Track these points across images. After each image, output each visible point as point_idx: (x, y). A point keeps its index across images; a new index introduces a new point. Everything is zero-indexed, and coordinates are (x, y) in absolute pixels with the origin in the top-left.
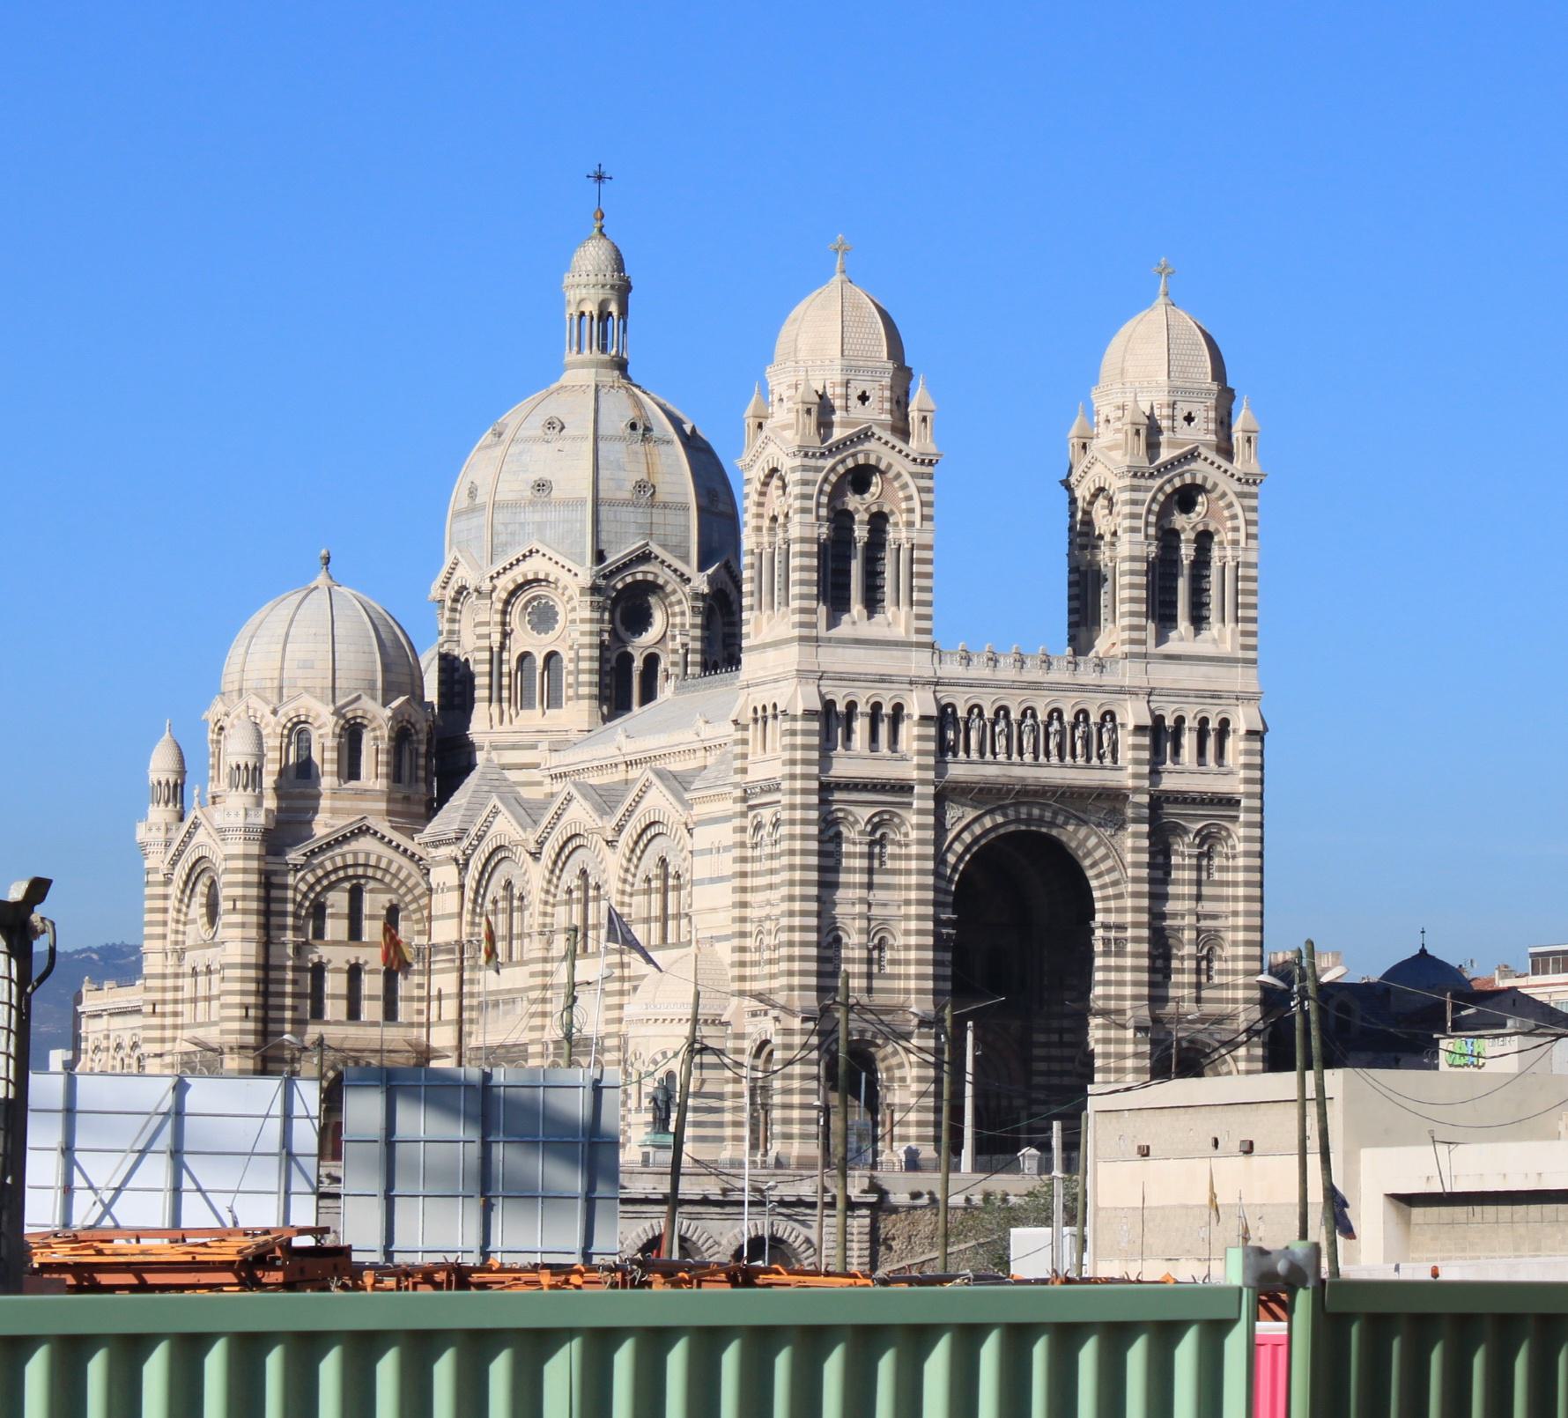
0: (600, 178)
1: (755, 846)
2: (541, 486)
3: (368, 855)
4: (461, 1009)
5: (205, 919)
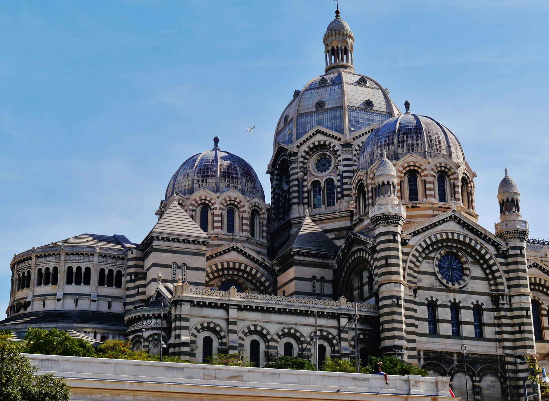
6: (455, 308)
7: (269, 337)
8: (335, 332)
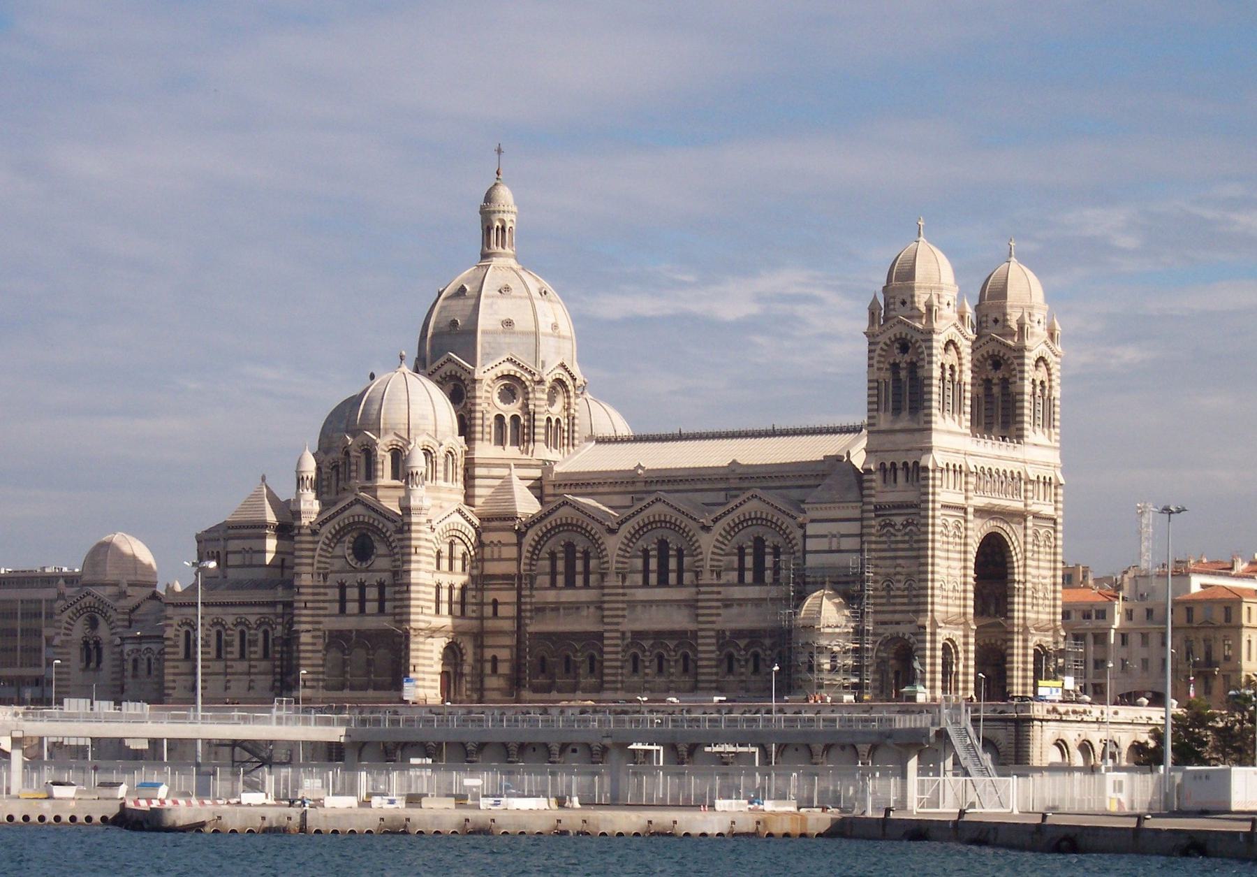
0: (499, 151)
1: (880, 536)
2: (509, 323)
3: (458, 524)
4: (519, 611)
5: (352, 557)
6: (362, 587)
7: (227, 627)
8: (272, 617)
